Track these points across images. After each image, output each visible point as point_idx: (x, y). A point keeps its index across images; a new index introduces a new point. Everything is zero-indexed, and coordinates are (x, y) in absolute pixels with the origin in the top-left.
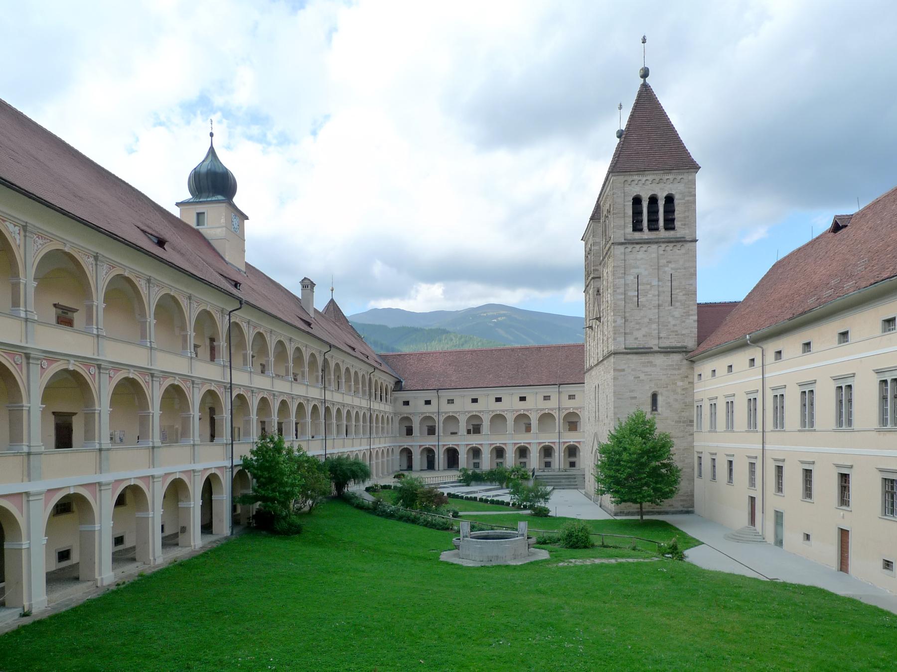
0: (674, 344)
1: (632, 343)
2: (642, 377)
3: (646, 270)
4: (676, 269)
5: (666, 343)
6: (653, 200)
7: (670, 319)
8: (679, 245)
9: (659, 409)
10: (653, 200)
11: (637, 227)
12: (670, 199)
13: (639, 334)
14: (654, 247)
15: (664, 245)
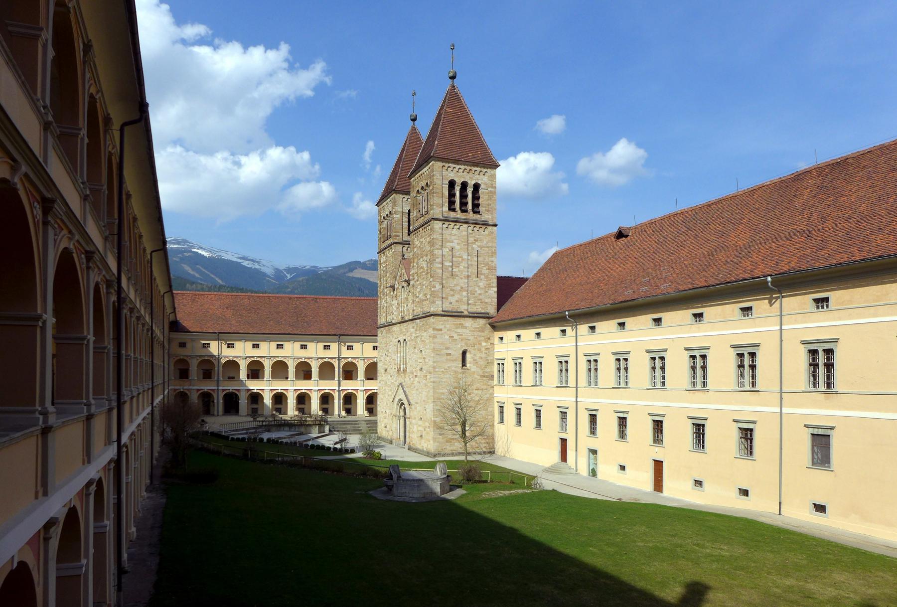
0: (480, 310)
1: (447, 307)
2: (456, 337)
3: (458, 244)
4: (481, 247)
5: (473, 309)
6: (464, 185)
7: (477, 289)
8: (484, 227)
9: (468, 365)
10: (464, 185)
11: (451, 208)
12: (476, 187)
13: (453, 299)
14: (466, 226)
15: (472, 226)
